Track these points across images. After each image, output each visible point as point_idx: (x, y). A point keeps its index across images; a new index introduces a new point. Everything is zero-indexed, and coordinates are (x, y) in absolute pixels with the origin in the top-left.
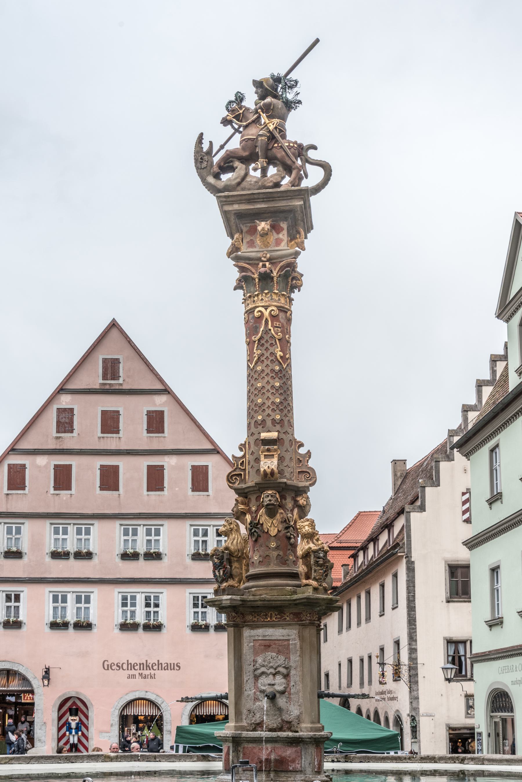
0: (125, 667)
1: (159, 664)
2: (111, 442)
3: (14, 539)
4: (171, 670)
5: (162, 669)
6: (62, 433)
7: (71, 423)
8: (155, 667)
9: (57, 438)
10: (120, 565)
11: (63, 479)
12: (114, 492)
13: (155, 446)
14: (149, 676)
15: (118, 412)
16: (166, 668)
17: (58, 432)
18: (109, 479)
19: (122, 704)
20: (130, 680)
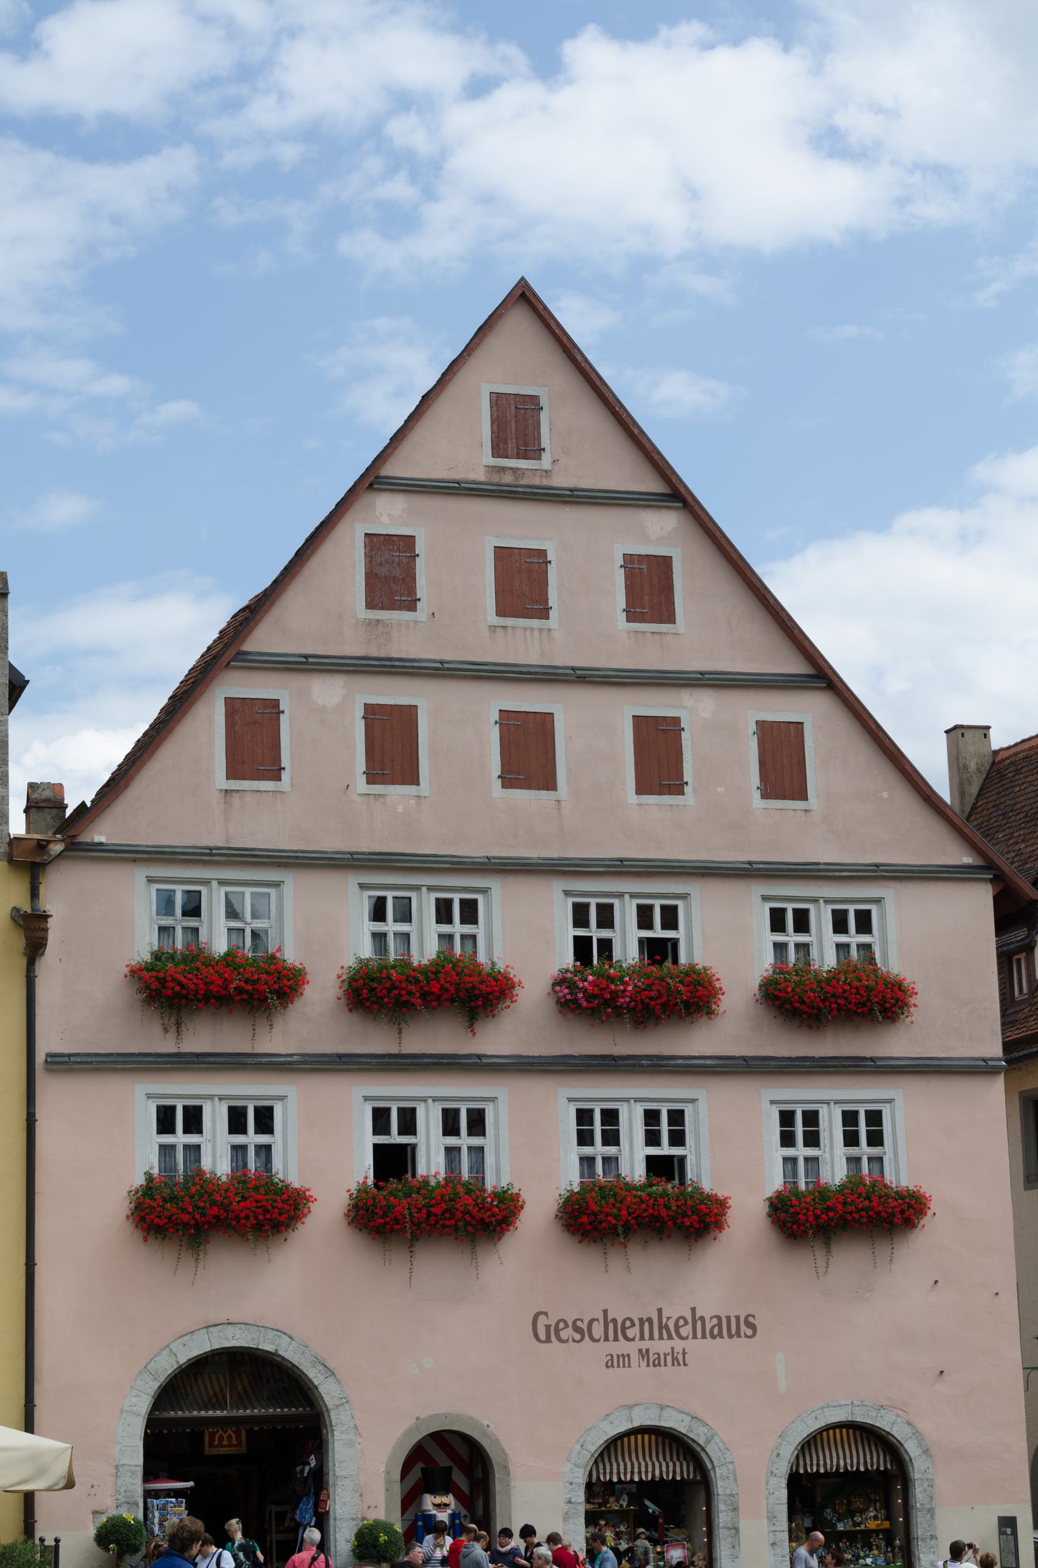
0: (598, 1330)
1: (696, 1318)
2: (524, 643)
4: (730, 1336)
5: (704, 1337)
11: (392, 749)
12: (544, 794)
13: (651, 660)
14: (669, 1359)
15: (543, 553)
16: (716, 1331)
17: (370, 605)
18: (528, 755)
19: (593, 1449)
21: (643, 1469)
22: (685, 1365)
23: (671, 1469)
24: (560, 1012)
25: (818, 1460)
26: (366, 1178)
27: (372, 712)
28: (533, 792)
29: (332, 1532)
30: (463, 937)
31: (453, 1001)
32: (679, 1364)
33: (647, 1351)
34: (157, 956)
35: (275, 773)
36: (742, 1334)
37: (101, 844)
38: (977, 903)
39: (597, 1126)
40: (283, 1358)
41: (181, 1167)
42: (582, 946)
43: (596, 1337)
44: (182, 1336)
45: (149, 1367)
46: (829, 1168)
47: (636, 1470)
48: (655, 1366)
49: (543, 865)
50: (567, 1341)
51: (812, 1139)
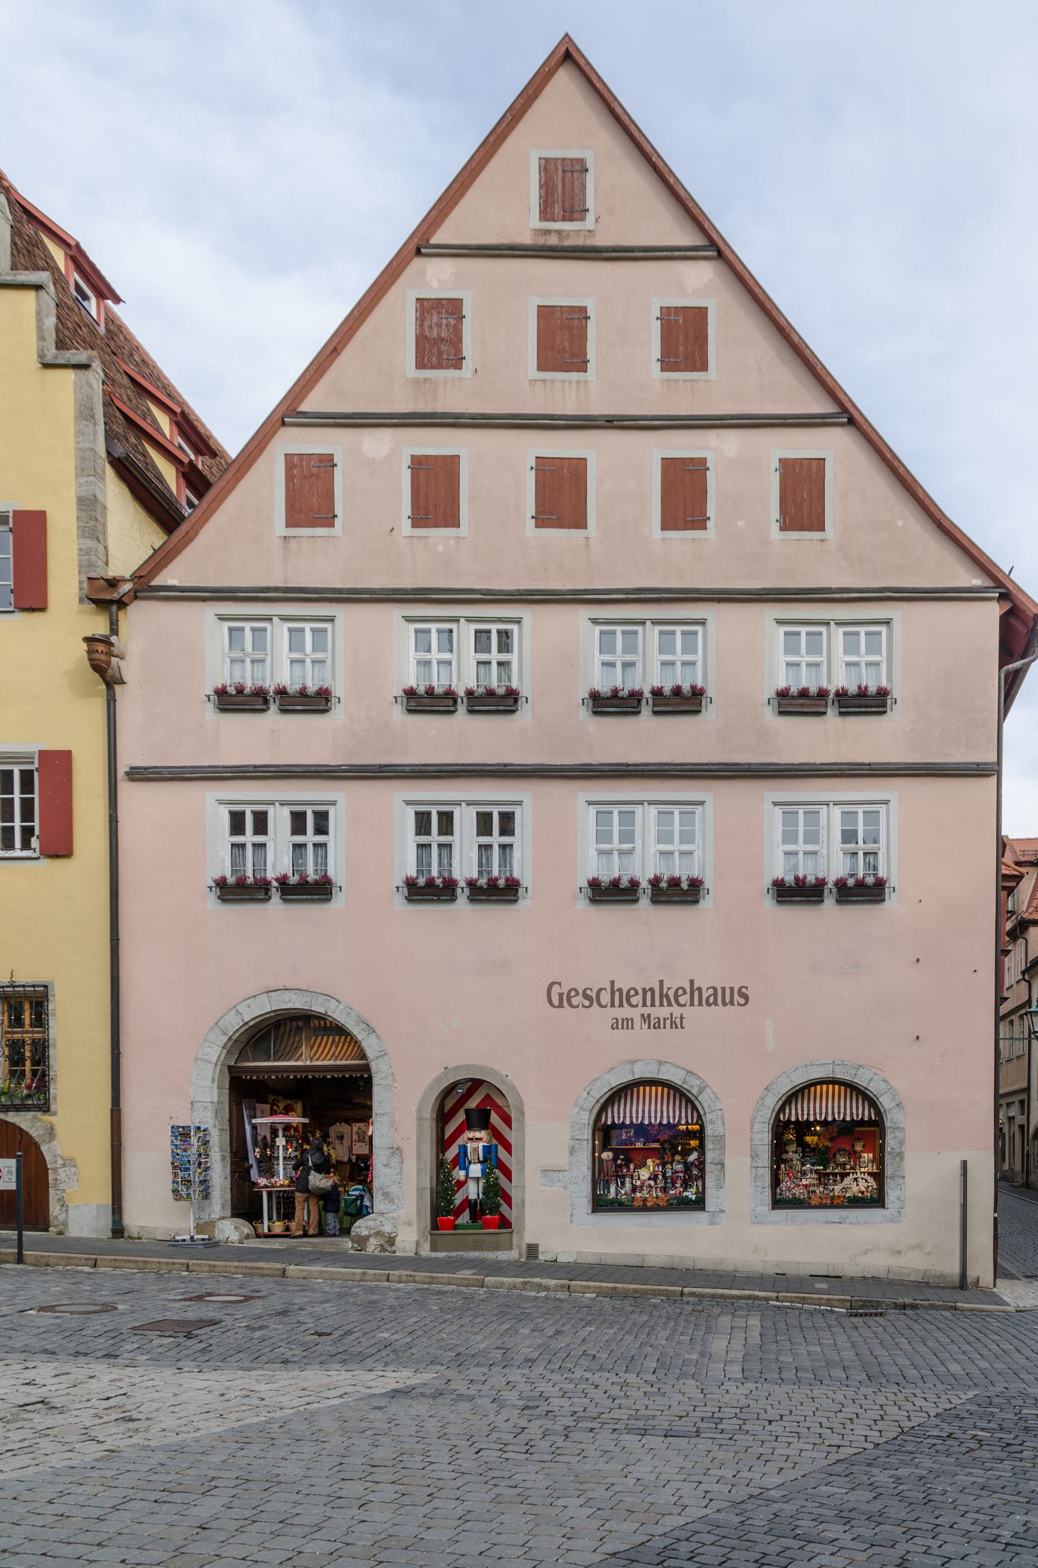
0: (605, 998)
1: (694, 990)
2: (564, 394)
3: (308, 661)
4: (724, 1004)
5: (700, 1004)
6: (432, 367)
9: (417, 382)
10: (591, 729)
12: (574, 533)
14: (668, 1022)
15: (583, 310)
16: (711, 1000)
17: (420, 365)
18: (561, 496)
20: (620, 1032)
22: (682, 1028)
27: (418, 463)
28: (563, 530)
32: (677, 1027)
33: (649, 1015)
36: (736, 1003)
43: (604, 1004)
48: (655, 1028)
50: (577, 1007)
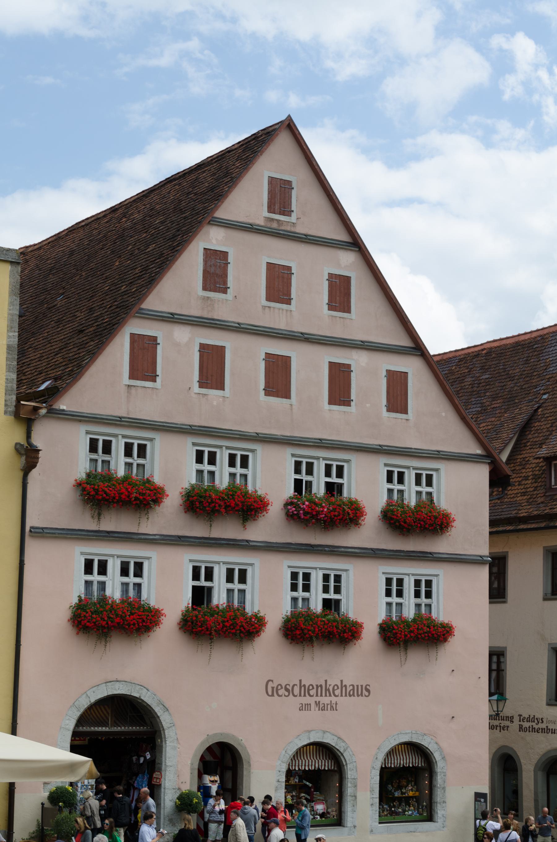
0: (296, 690)
1: (343, 686)
2: (278, 317)
4: (358, 696)
5: (346, 696)
6: (210, 291)
7: (224, 276)
8: (338, 692)
12: (284, 400)
13: (338, 332)
14: (329, 706)
16: (351, 693)
17: (205, 288)
20: (303, 712)
21: (310, 764)
22: (336, 710)
23: (323, 764)
24: (287, 519)
25: (391, 761)
26: (188, 604)
27: (203, 348)
29: (162, 796)
30: (241, 475)
31: (239, 511)
33: (319, 702)
34: (88, 475)
35: (153, 379)
37: (63, 410)
38: (480, 475)
39: (300, 581)
40: (143, 701)
41: (96, 594)
42: (298, 484)
43: (296, 694)
44: (93, 687)
45: (75, 704)
46: (407, 609)
47: (307, 764)
48: (322, 710)
49: (284, 439)
50: (281, 696)
51: (400, 594)
